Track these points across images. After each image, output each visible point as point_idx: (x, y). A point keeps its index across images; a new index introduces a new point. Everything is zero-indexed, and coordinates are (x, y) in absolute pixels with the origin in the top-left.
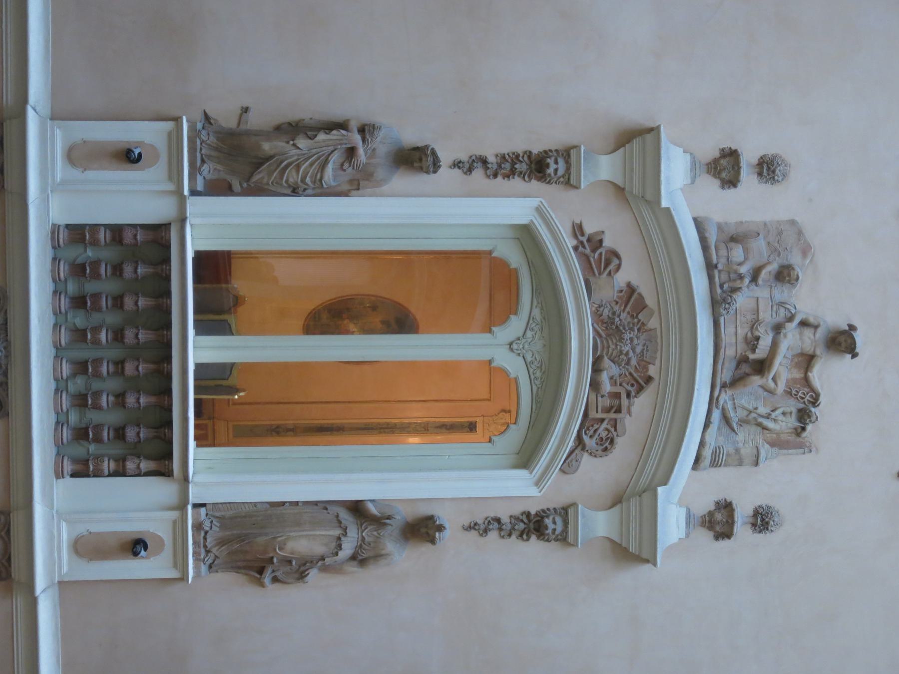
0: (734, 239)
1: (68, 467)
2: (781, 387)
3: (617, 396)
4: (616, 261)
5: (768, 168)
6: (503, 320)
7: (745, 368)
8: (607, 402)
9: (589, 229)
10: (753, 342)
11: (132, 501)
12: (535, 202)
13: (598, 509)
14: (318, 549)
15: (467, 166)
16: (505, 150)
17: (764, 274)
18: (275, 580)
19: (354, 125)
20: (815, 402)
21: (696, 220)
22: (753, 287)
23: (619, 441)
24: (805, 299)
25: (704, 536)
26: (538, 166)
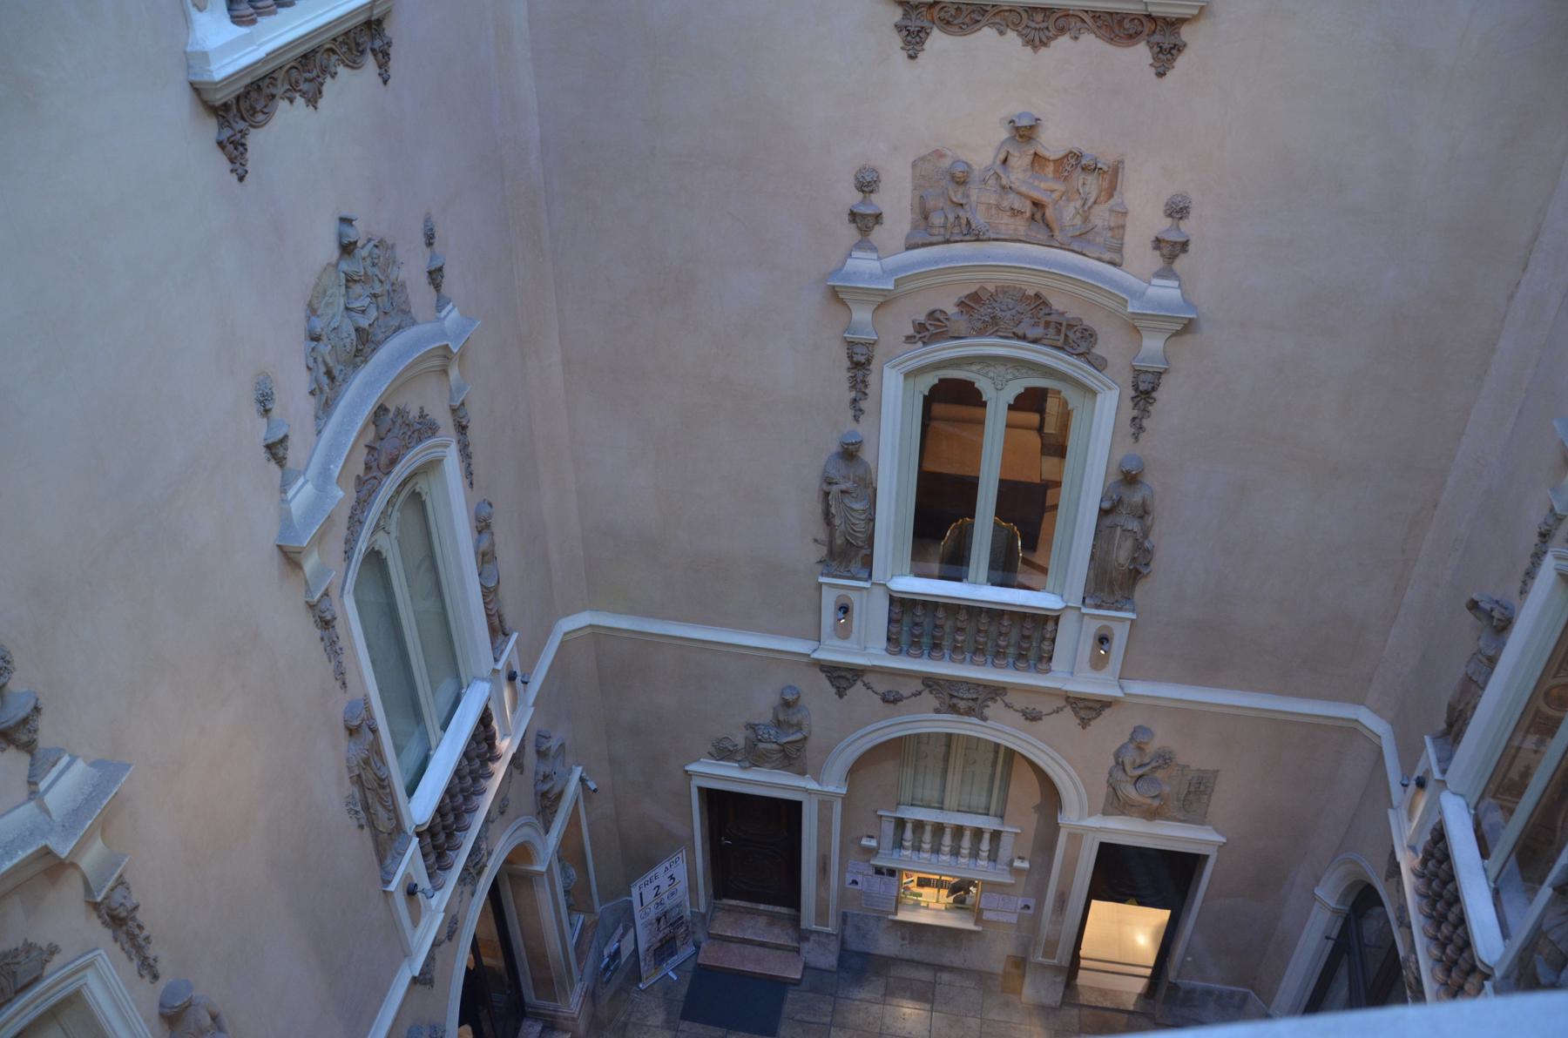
0: (926, 218)
1: (1042, 666)
2: (1060, 187)
3: (1047, 324)
4: (938, 315)
5: (867, 185)
6: (978, 393)
7: (1038, 216)
8: (1052, 331)
9: (911, 331)
10: (1015, 212)
11: (1072, 641)
12: (886, 370)
13: (1140, 345)
14: (1129, 544)
15: (858, 413)
16: (847, 385)
17: (958, 198)
18: (1147, 565)
19: (826, 488)
20: (1079, 156)
21: (907, 249)
22: (967, 208)
23: (1086, 323)
24: (982, 157)
25: (1181, 264)
26: (860, 365)
